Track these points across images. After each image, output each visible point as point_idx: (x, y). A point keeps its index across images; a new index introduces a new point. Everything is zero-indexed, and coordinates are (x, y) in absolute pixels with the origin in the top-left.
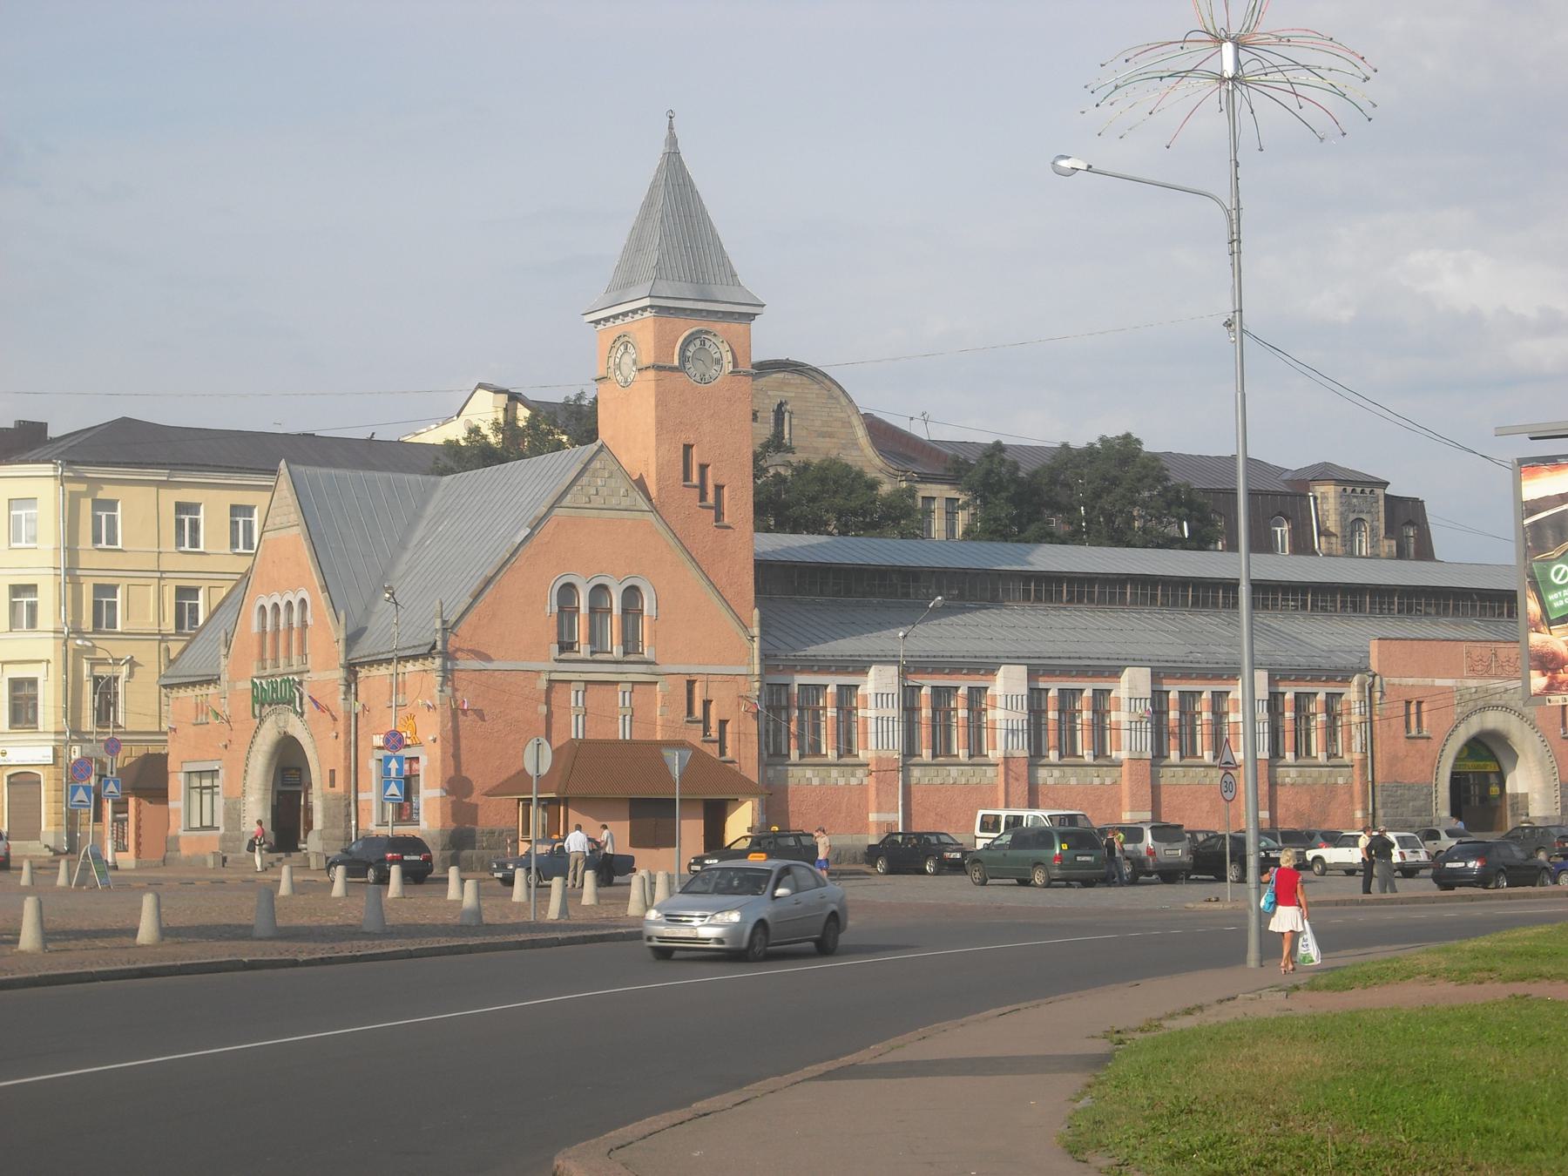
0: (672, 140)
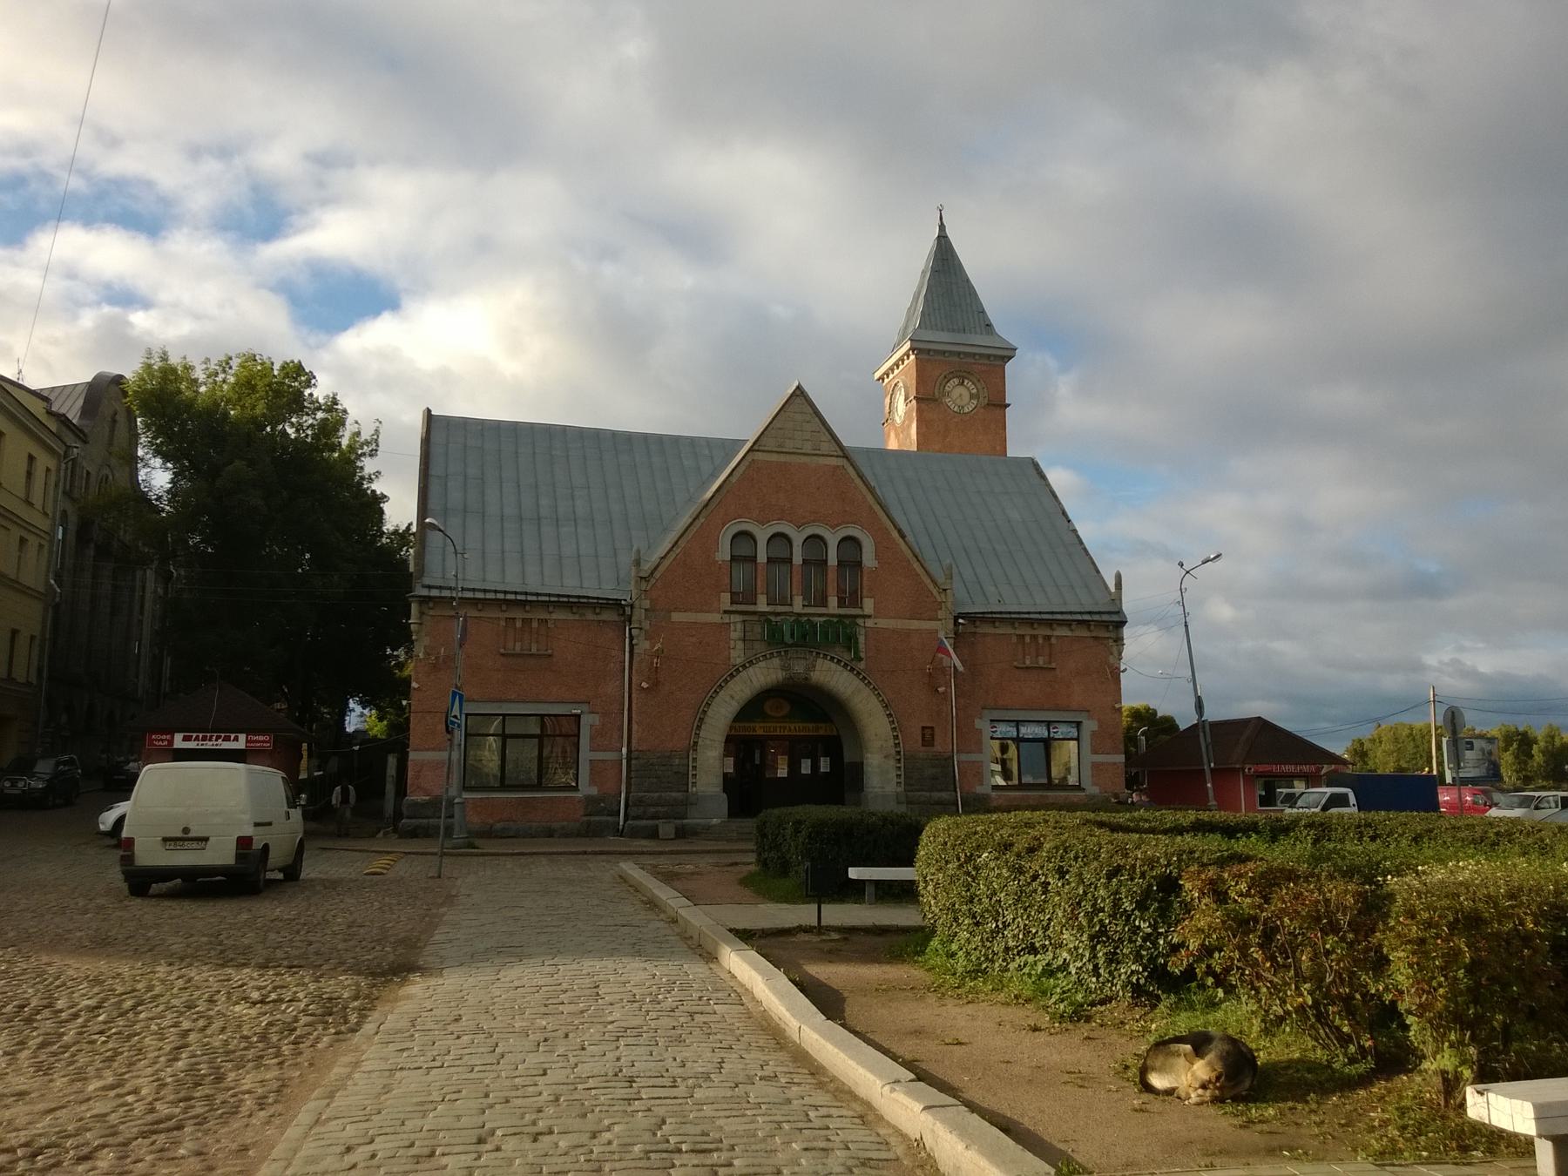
0: (942, 227)
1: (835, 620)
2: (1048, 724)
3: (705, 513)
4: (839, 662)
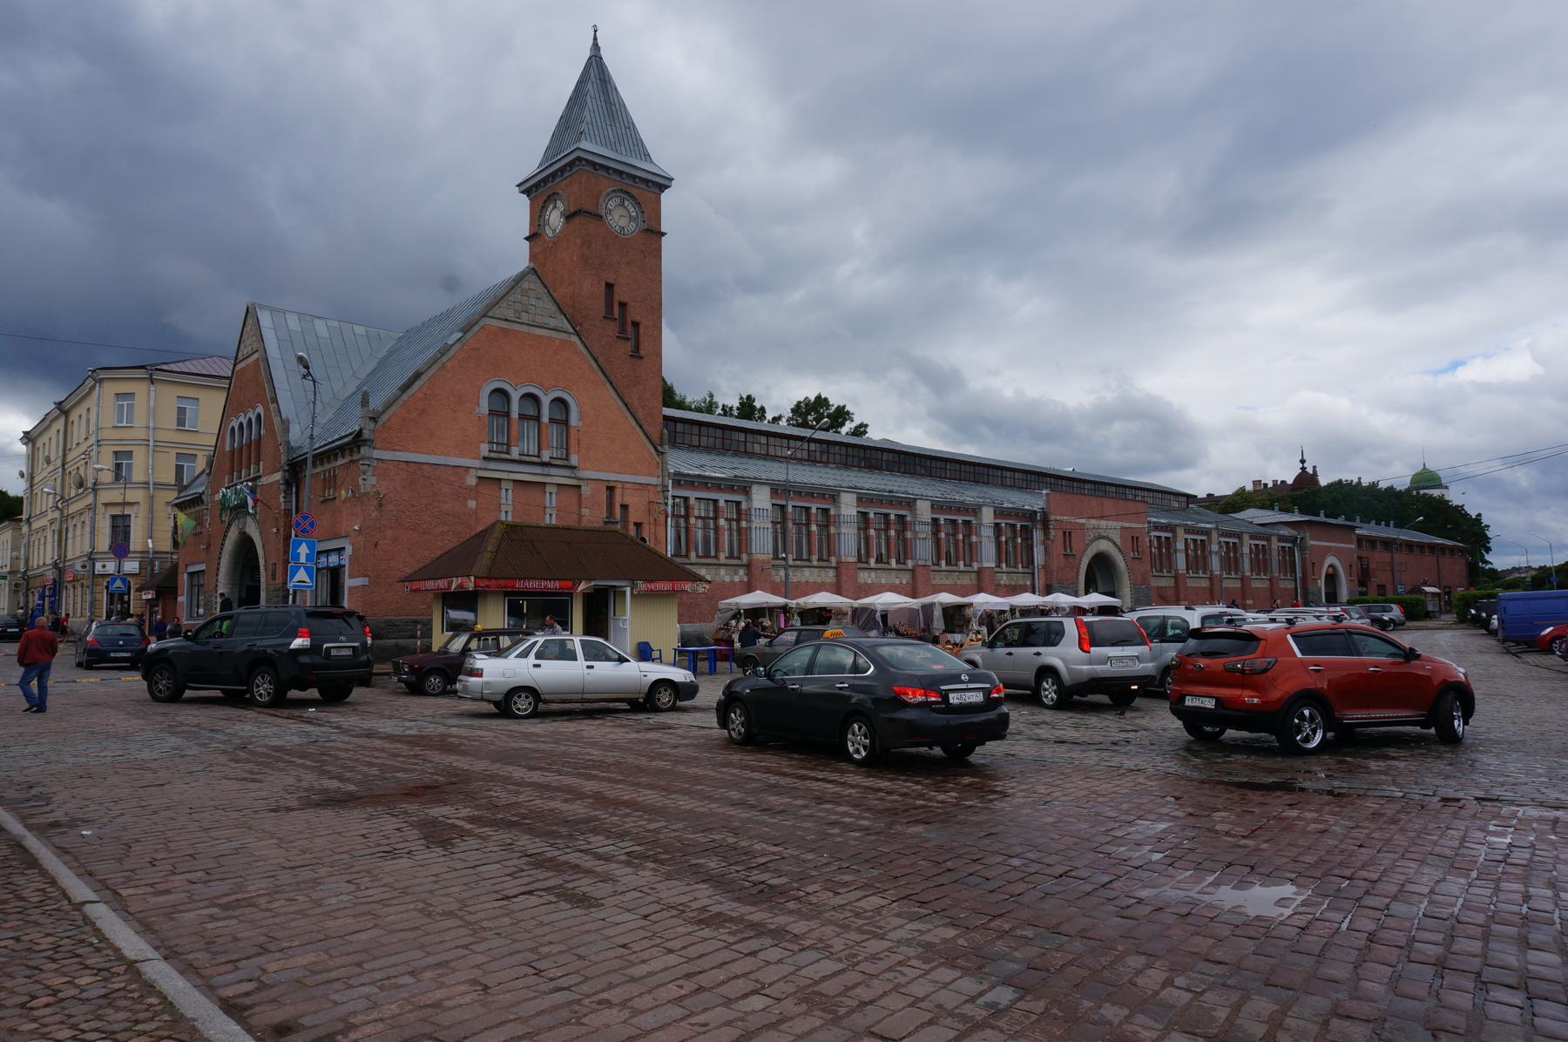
0: (596, 46)
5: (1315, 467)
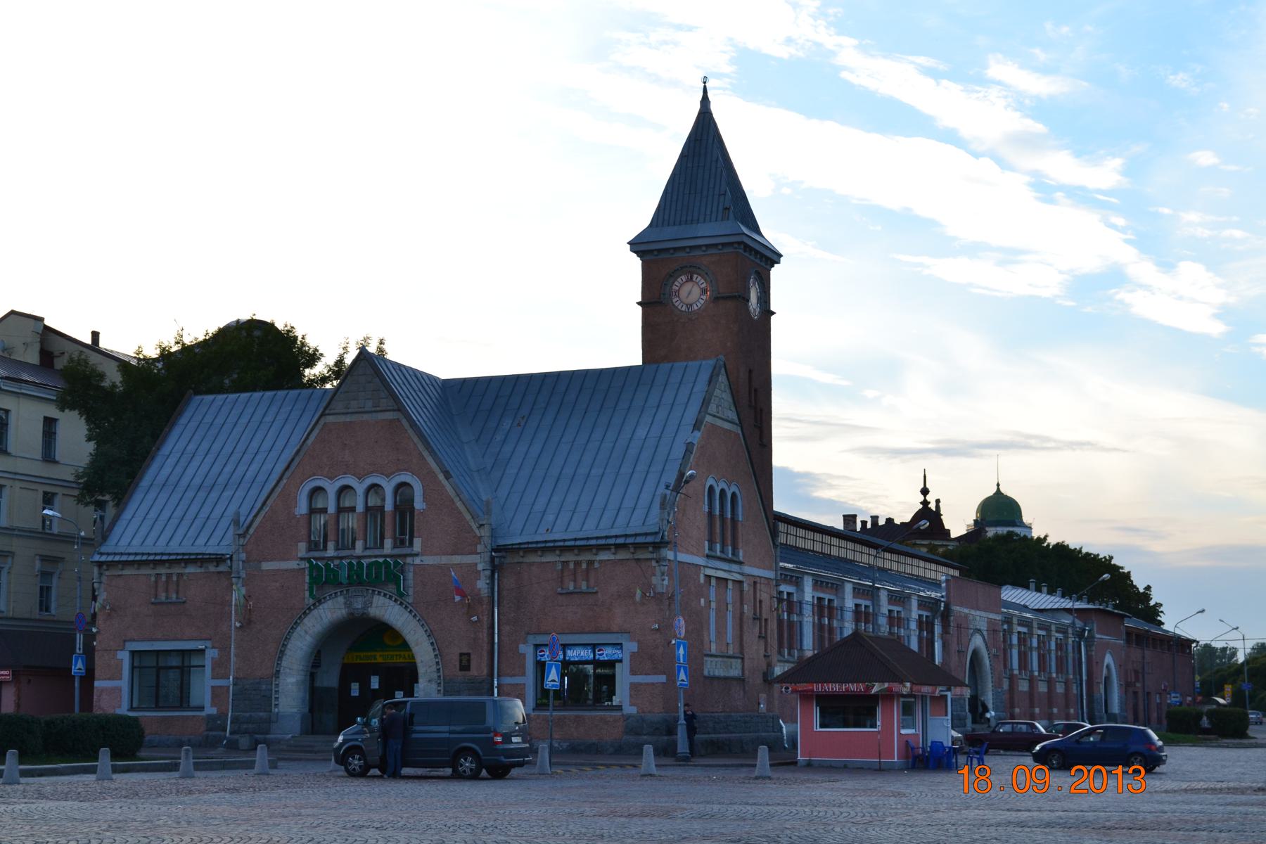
0: (705, 101)
1: (381, 560)
2: (594, 646)
3: (288, 474)
4: (390, 598)
5: (938, 501)
